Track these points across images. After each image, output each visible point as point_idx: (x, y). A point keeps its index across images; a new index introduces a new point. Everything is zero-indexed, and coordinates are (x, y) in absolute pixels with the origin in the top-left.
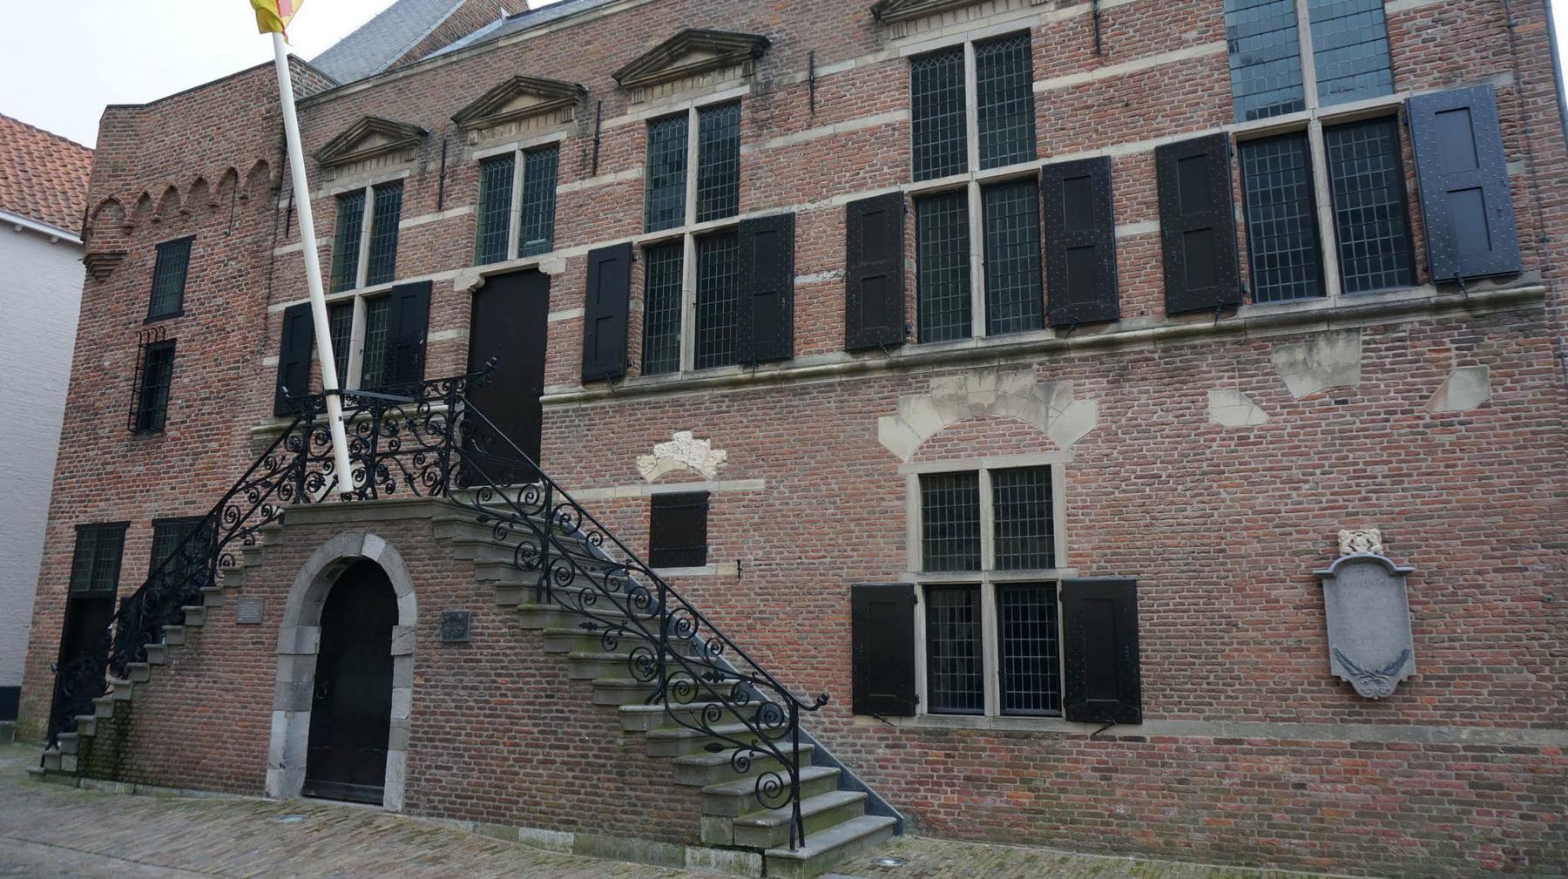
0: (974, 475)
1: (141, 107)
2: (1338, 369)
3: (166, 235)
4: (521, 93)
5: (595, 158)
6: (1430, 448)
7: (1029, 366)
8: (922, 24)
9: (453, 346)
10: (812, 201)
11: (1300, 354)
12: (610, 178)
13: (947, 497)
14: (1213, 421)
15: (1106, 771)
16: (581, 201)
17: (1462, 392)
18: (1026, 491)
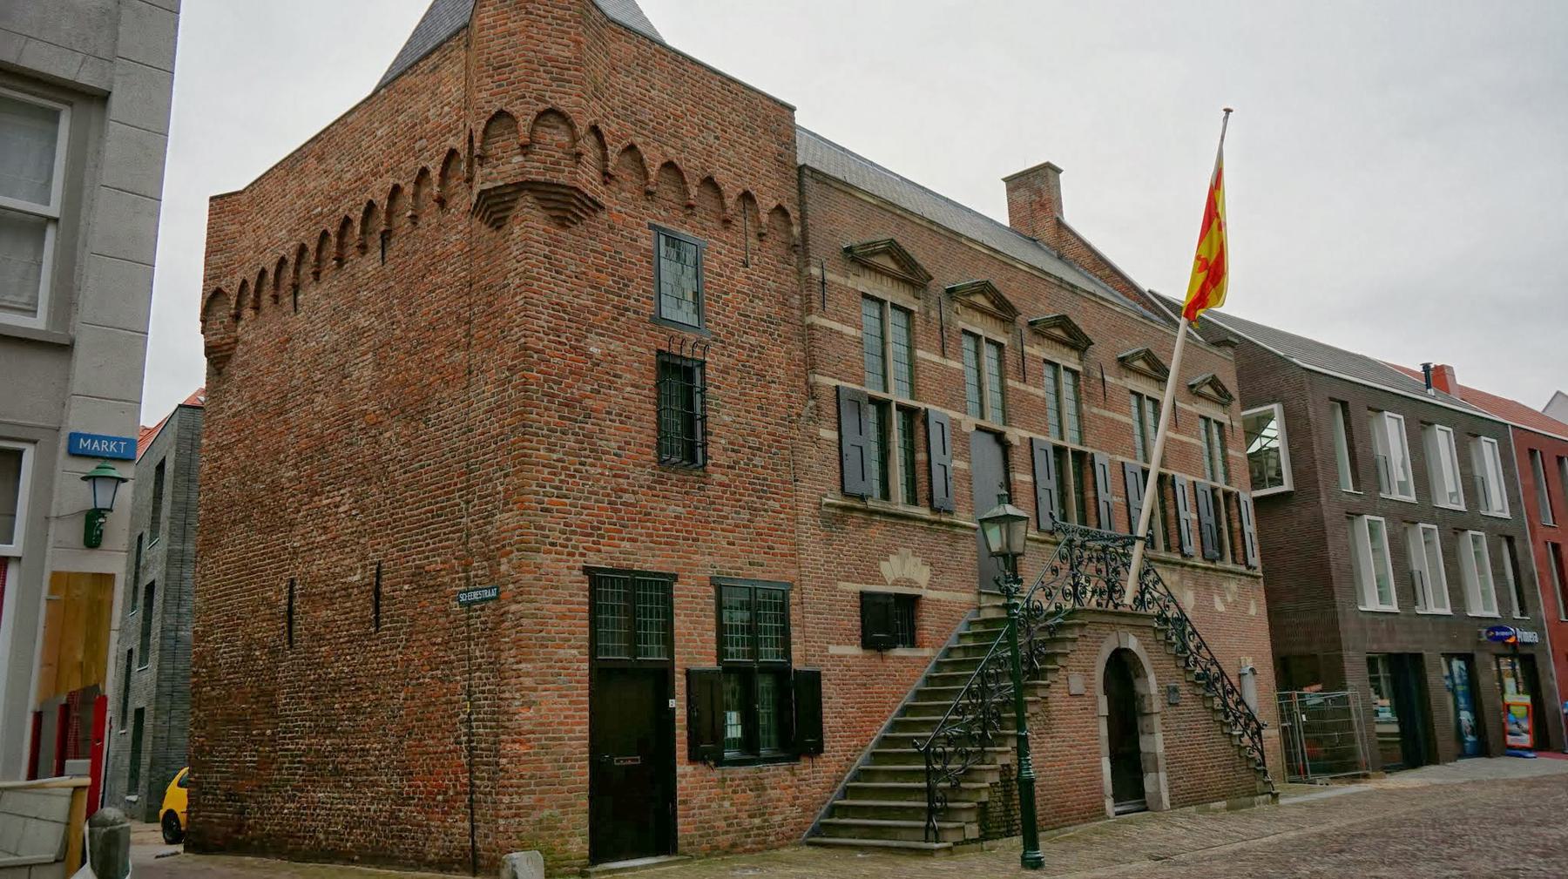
4: (982, 293)
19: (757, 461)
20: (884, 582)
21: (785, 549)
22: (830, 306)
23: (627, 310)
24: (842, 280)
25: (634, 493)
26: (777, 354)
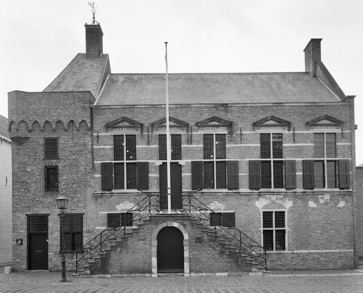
0: (272, 212)
1: (28, 93)
2: (327, 199)
3: (47, 135)
5: (191, 141)
6: (337, 212)
7: (281, 195)
8: (263, 128)
9: (156, 178)
10: (242, 159)
11: (322, 196)
12: (195, 146)
13: (267, 216)
14: (309, 206)
15: (292, 258)
16: (189, 150)
17: (342, 204)
18: (281, 215)
19: (74, 186)
20: (117, 210)
21: (82, 205)
22: (100, 142)
23: (37, 159)
24: (105, 134)
25: (38, 198)
26: (82, 159)
